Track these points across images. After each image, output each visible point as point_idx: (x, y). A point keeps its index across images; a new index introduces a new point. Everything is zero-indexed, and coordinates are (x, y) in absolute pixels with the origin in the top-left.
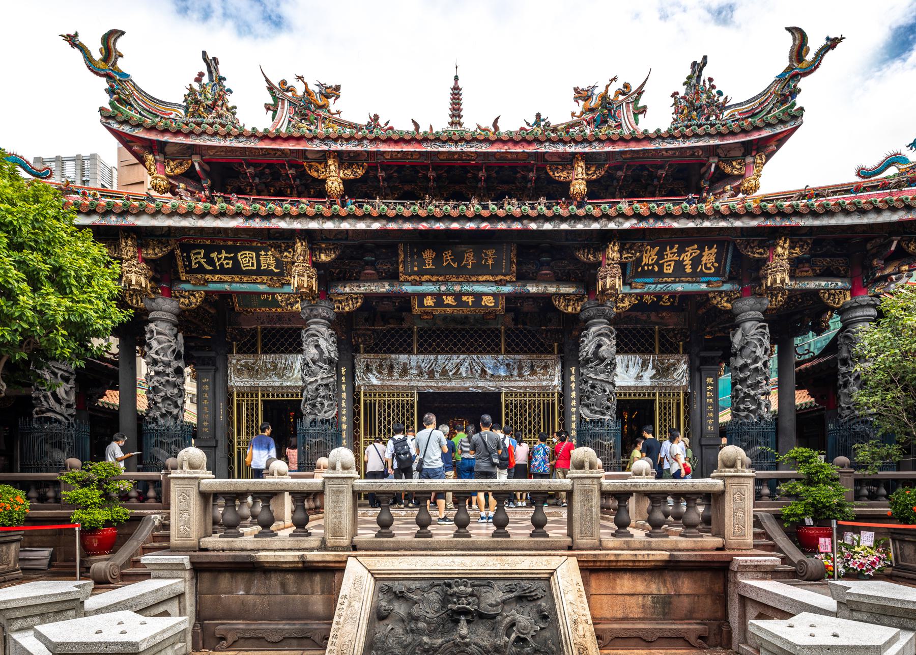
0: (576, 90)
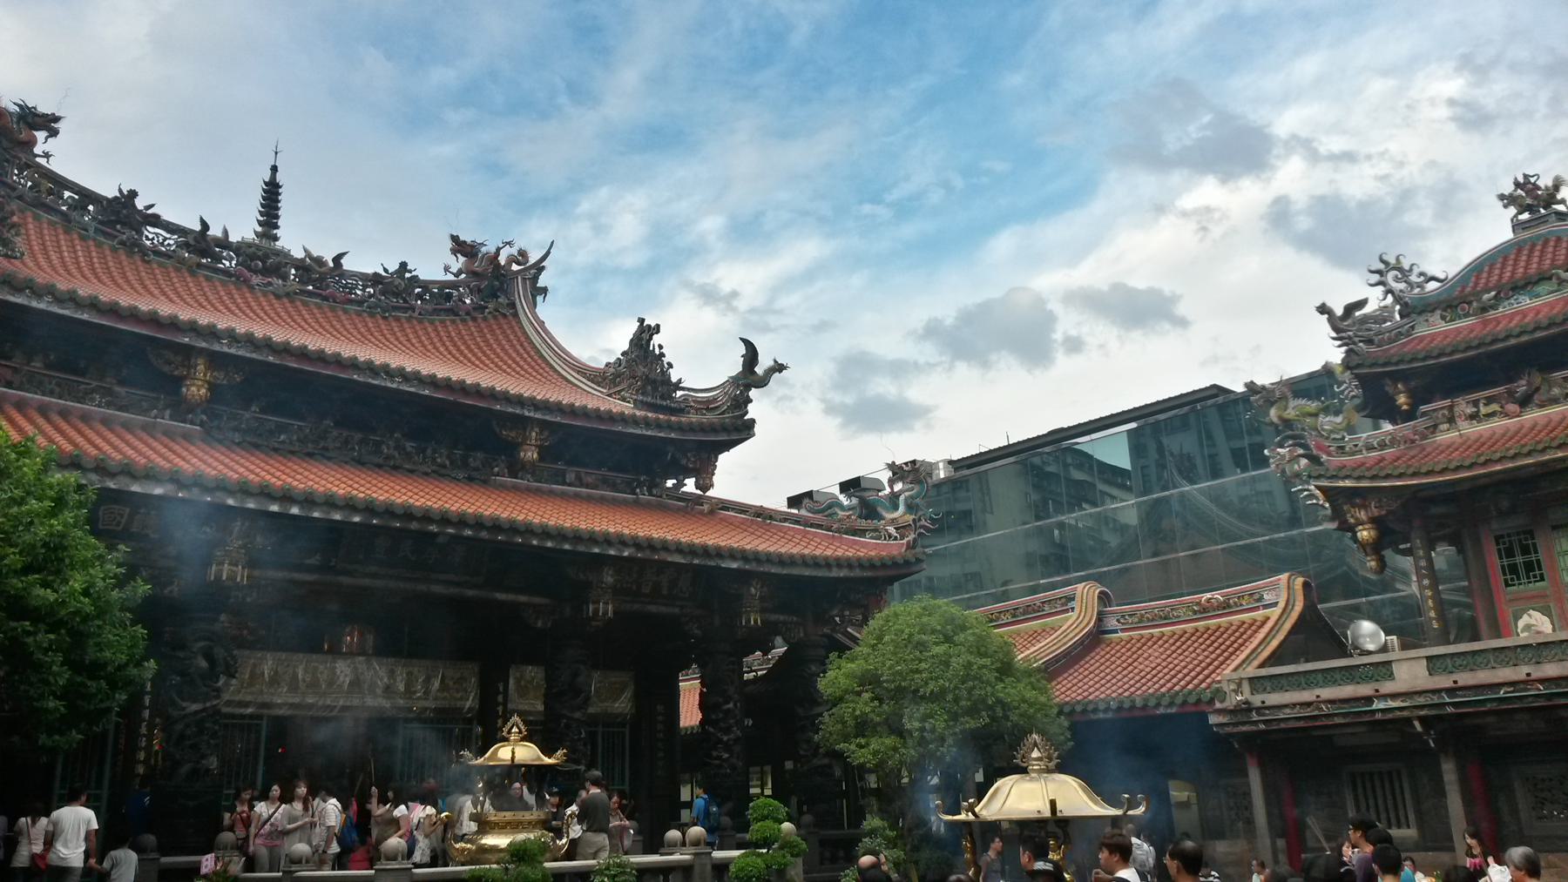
0: (455, 239)
